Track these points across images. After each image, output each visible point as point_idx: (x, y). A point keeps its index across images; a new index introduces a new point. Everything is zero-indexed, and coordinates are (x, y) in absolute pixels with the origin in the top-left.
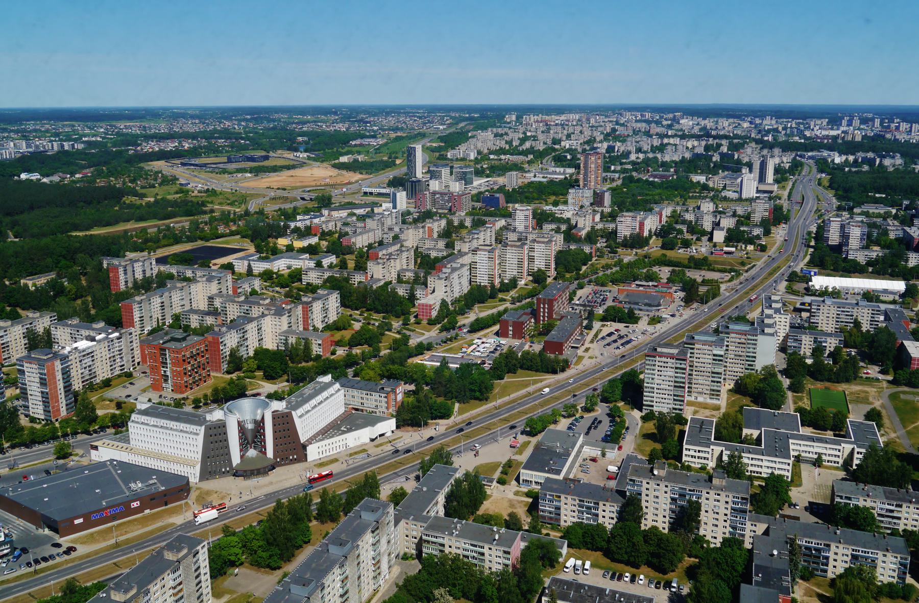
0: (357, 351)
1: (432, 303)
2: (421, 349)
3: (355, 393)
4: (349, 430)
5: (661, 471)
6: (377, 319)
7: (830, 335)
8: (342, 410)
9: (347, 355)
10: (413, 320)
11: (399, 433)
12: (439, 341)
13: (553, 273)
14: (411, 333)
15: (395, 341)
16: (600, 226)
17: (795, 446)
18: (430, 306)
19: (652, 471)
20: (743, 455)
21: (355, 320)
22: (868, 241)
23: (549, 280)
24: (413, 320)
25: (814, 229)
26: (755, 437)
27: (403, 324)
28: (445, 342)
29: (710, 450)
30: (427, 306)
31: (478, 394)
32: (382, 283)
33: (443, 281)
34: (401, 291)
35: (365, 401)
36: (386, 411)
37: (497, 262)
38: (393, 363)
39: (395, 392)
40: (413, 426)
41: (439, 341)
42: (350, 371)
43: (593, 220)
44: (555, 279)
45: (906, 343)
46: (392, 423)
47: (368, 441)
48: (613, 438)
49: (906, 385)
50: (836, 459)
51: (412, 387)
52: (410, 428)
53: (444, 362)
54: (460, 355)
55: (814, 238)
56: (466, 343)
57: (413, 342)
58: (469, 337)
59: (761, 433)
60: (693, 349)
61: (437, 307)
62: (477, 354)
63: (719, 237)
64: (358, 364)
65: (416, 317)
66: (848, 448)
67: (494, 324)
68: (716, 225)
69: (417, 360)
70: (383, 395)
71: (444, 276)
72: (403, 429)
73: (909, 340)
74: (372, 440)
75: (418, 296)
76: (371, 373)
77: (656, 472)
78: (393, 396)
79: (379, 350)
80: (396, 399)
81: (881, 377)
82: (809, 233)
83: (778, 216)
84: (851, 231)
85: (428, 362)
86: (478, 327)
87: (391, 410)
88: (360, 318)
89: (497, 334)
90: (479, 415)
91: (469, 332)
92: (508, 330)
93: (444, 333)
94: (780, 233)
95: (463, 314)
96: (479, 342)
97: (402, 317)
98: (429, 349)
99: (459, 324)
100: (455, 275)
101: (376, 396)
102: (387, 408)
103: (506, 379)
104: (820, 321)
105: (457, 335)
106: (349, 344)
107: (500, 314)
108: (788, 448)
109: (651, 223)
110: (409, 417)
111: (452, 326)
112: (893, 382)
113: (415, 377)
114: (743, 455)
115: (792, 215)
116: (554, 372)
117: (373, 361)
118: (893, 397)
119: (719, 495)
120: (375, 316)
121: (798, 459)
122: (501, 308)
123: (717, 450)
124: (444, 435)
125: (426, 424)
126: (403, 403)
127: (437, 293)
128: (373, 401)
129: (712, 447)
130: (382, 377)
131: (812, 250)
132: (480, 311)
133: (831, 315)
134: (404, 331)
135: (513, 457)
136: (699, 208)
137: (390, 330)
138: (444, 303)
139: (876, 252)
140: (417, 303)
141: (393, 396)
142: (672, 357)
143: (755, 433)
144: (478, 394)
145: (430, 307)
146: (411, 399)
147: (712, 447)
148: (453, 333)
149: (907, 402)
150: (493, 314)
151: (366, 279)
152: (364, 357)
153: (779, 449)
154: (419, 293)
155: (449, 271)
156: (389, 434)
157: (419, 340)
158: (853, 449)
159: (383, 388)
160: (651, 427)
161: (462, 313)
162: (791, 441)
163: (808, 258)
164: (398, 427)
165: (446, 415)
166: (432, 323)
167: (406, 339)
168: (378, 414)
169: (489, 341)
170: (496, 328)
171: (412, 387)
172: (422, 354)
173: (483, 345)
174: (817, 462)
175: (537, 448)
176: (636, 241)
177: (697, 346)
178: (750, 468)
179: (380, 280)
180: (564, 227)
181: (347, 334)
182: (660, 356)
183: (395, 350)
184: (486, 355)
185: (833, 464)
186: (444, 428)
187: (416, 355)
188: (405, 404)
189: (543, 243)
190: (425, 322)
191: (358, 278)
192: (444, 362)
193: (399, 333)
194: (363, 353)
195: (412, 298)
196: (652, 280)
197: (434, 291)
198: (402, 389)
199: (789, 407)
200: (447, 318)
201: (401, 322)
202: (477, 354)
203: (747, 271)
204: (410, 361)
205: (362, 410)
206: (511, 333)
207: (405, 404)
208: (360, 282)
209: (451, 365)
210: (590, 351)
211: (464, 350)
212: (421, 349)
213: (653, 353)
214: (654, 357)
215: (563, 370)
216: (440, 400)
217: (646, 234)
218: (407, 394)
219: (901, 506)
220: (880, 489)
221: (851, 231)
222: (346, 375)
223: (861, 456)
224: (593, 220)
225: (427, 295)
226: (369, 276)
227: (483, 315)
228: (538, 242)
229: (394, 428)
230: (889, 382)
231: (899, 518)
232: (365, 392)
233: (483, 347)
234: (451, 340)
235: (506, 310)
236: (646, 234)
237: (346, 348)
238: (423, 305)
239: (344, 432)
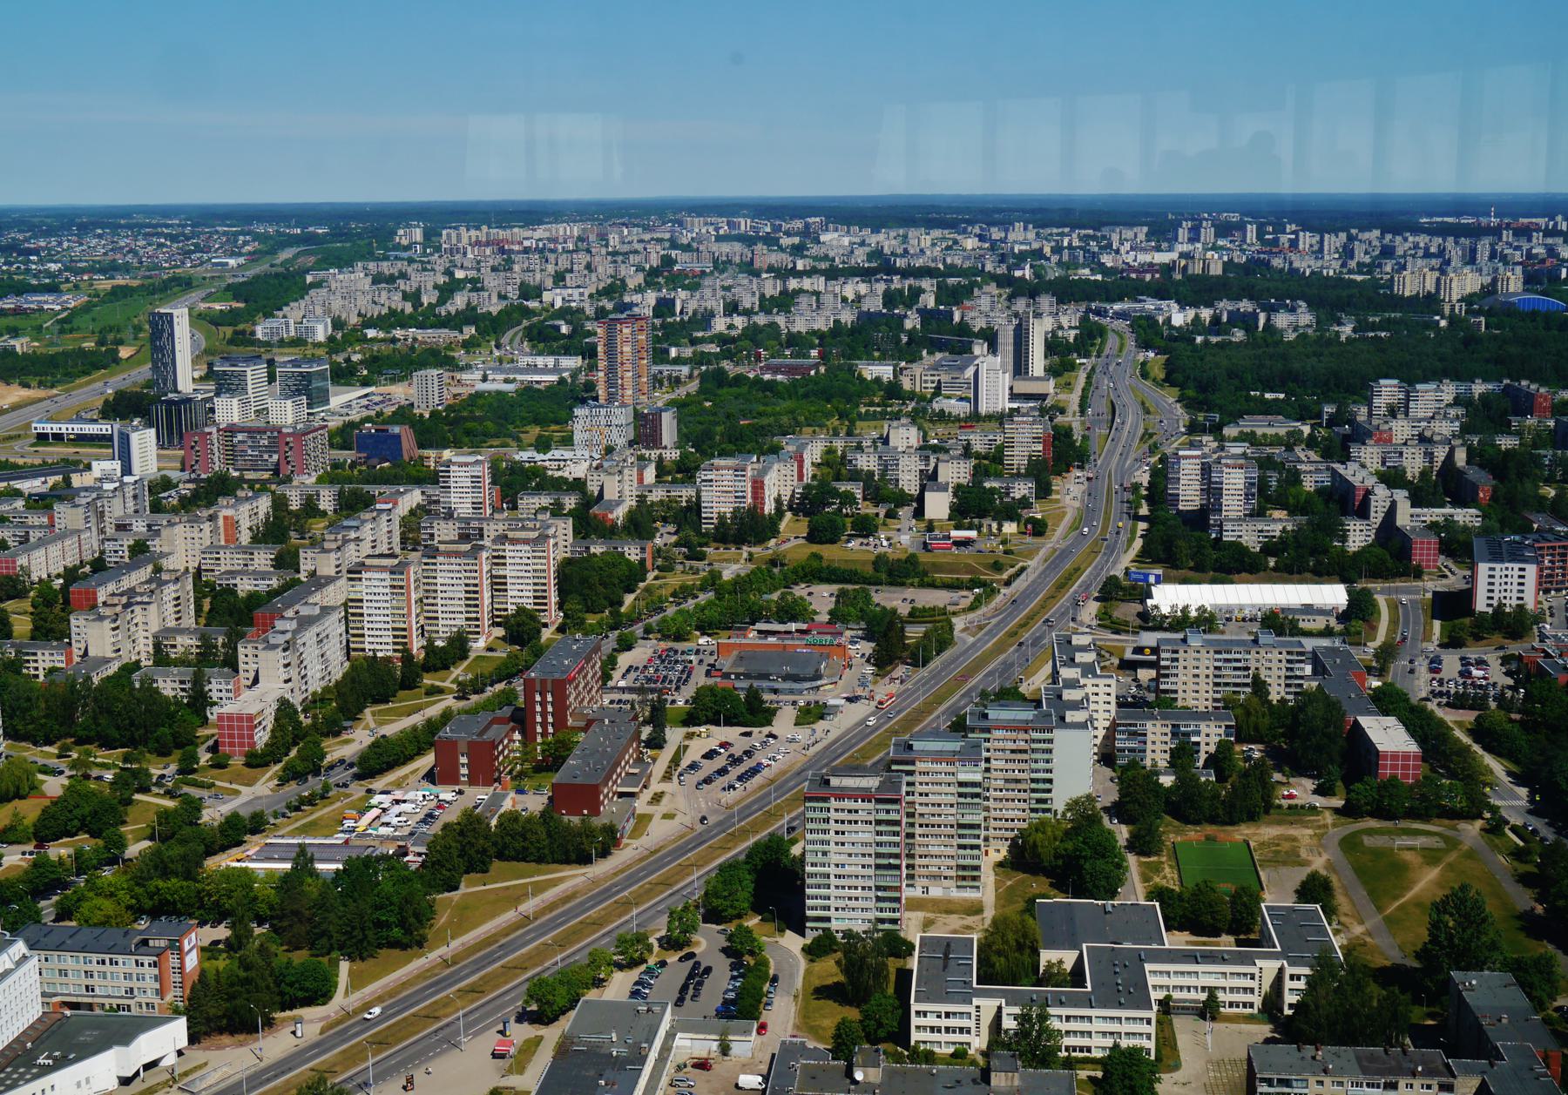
0: (59, 851)
1: (253, 710)
2: (235, 832)
3: (69, 961)
4: (61, 1063)
5: (871, 1070)
6: (107, 764)
7: (1204, 716)
8: (34, 1011)
9: (35, 865)
10: (204, 757)
11: (198, 1055)
12: (281, 807)
13: (553, 616)
14: (205, 793)
15: (164, 815)
16: (657, 495)
17: (1160, 979)
18: (250, 718)
19: (849, 1073)
20: (1052, 1011)
21: (46, 770)
22: (1263, 500)
23: (546, 634)
24: (204, 757)
25: (1145, 479)
26: (1068, 966)
27: (180, 772)
28: (297, 809)
29: (972, 1010)
30: (240, 718)
31: (397, 932)
32: (113, 668)
33: (279, 653)
34: (169, 686)
35: (96, 981)
36: (157, 1001)
37: (414, 596)
38: (165, 873)
39: (180, 949)
40: (232, 1034)
41: (281, 807)
42: (47, 907)
43: (641, 480)
44: (561, 629)
45: (1364, 721)
46: (177, 1030)
47: (113, 1084)
48: (744, 1008)
49: (1373, 815)
50: (1248, 998)
51: (222, 932)
52: (226, 1039)
53: (303, 859)
54: (339, 839)
55: (1147, 498)
56: (352, 806)
57: (213, 814)
58: (357, 790)
59: (1081, 956)
60: (911, 773)
61: (269, 722)
62: (383, 831)
63: (938, 505)
64: (65, 886)
65: (214, 749)
66: (1269, 967)
67: (420, 752)
68: (930, 479)
69: (226, 861)
70: (146, 960)
71: (281, 639)
72: (206, 1043)
73: (1369, 713)
74: (125, 1082)
75: (215, 696)
76: (108, 906)
77: (859, 1076)
78: (173, 961)
79: (122, 845)
80: (182, 967)
81: (1319, 801)
82: (1136, 487)
83: (1063, 453)
84: (1220, 478)
85: (257, 861)
86: (380, 761)
87: (169, 998)
88: (62, 764)
89: (430, 777)
90: (405, 985)
91: (359, 777)
92: (456, 766)
93: (292, 788)
94: (1071, 490)
95: (337, 734)
96: (386, 800)
97: (177, 754)
98: (254, 832)
99: (329, 758)
100: (309, 636)
101: (127, 963)
102: (161, 993)
103: (464, 889)
104: (1180, 687)
105: (326, 788)
106: (36, 835)
107: (432, 727)
109: (780, 482)
110: (220, 1012)
111: (312, 765)
112: (1345, 812)
113: (228, 904)
114: (1052, 1011)
115: (1094, 446)
116: (585, 859)
117: (107, 873)
118: (1349, 844)
120: (102, 755)
121: (1166, 1006)
122: (434, 711)
123: (988, 1006)
124: (319, 1047)
125: (269, 1023)
126: (203, 973)
127: (264, 685)
128: (119, 978)
129: (976, 1001)
130: (138, 912)
131: (1142, 526)
132: (381, 724)
133: (1202, 672)
134: (186, 789)
135: (504, 1082)
136: (886, 441)
137: (145, 790)
138: (284, 707)
139: (1279, 523)
140: (213, 714)
141: (173, 961)
142: (866, 796)
143: (1068, 958)
144: (397, 932)
145: (250, 722)
146: (222, 963)
147: (976, 1001)
148: (314, 784)
149: (1377, 853)
150: (414, 728)
151: (69, 660)
152: (81, 864)
153: (1124, 988)
154: (216, 687)
155: (293, 625)
156: (170, 1060)
157: (226, 808)
158: (1281, 970)
159: (145, 942)
160: (829, 970)
161: (334, 729)
162: (1148, 967)
163: (1138, 544)
164: (193, 1039)
165: (319, 994)
166: (257, 761)
167: (195, 807)
168: (135, 1011)
169: (410, 796)
170: (427, 761)
171: (222, 932)
172: (239, 843)
173: (397, 809)
174: (1208, 1010)
175: (564, 1050)
176: (749, 527)
177: (920, 766)
178: (1068, 1041)
179: (107, 661)
180: (570, 502)
181: (29, 810)
182: (840, 798)
183: (164, 839)
184: (406, 831)
185: (1241, 1010)
186: (317, 1027)
187: (224, 849)
188: (211, 976)
189: (526, 542)
190: (237, 761)
191: (45, 660)
192: (303, 859)
193: (170, 794)
194: (78, 855)
195: (199, 701)
196: (793, 619)
197: (256, 681)
198: (197, 938)
199: (1134, 891)
200: (297, 741)
201: (173, 768)
202: (383, 831)
203: (1008, 583)
204: (212, 863)
205: (90, 1007)
206: (464, 771)
207: (211, 976)
208: (51, 671)
209: (319, 866)
210: (665, 800)
211: (349, 823)
212: (235, 832)
213: (822, 792)
214: (826, 800)
215: (605, 853)
216: (300, 957)
217: (769, 507)
218: (209, 951)
220: (1348, 1052)
221: (1220, 478)
222: (36, 918)
224: (641, 480)
225: (237, 692)
226: (76, 654)
227: (390, 730)
228: (514, 541)
229: (183, 1042)
230: (1336, 811)
232: (95, 957)
233: (401, 811)
234: (310, 801)
235: (447, 716)
236: (769, 507)
237: (30, 847)
238: (230, 718)
239: (46, 1070)
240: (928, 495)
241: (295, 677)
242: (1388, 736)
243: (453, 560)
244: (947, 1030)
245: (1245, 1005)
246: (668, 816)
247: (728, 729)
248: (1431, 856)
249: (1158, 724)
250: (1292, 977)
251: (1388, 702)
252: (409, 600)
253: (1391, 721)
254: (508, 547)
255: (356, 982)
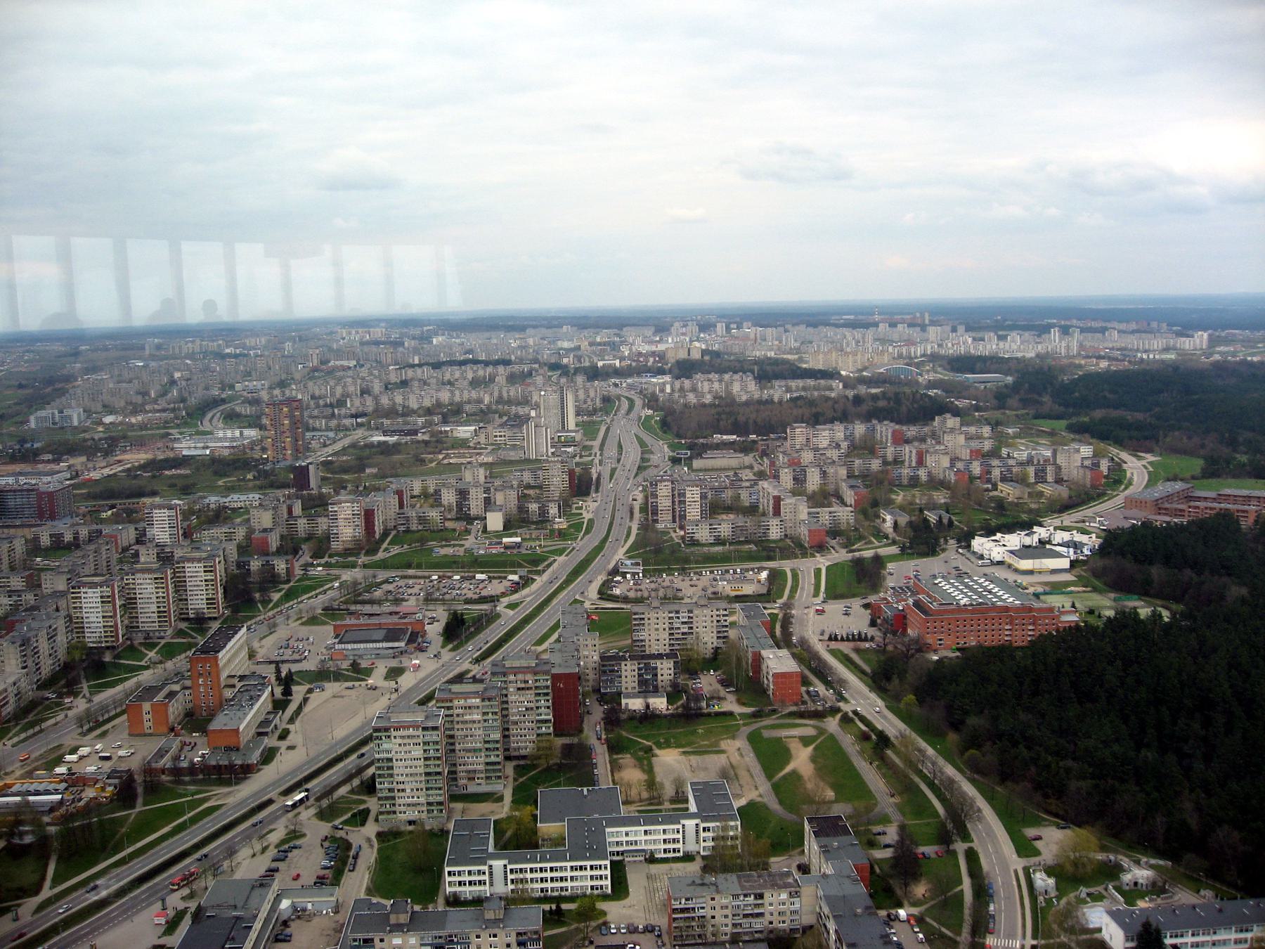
7: (660, 656)
16: (302, 525)
22: (714, 509)
25: (640, 497)
29: (485, 868)
45: (764, 653)
48: (332, 877)
63: (495, 521)
68: (488, 503)
81: (738, 709)
104: (647, 638)
108: (603, 844)
118: (754, 739)
119: (495, 936)
133: (661, 626)
142: (415, 726)
149: (770, 740)
153: (587, 844)
162: (608, 830)
182: (397, 729)
189: (199, 560)
210: (290, 737)
219: (761, 896)
223: (710, 834)
228: (192, 560)
231: (762, 915)
240: (488, 514)
241: (30, 663)
242: (778, 662)
243: (146, 576)
244: (470, 883)
245: (674, 850)
246: (291, 748)
247: (337, 684)
248: (806, 741)
249: (629, 663)
250: (704, 829)
251: (784, 641)
252: (114, 606)
253: (784, 653)
254: (187, 565)
255: (56, 881)
